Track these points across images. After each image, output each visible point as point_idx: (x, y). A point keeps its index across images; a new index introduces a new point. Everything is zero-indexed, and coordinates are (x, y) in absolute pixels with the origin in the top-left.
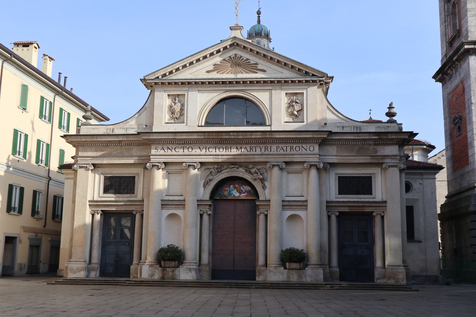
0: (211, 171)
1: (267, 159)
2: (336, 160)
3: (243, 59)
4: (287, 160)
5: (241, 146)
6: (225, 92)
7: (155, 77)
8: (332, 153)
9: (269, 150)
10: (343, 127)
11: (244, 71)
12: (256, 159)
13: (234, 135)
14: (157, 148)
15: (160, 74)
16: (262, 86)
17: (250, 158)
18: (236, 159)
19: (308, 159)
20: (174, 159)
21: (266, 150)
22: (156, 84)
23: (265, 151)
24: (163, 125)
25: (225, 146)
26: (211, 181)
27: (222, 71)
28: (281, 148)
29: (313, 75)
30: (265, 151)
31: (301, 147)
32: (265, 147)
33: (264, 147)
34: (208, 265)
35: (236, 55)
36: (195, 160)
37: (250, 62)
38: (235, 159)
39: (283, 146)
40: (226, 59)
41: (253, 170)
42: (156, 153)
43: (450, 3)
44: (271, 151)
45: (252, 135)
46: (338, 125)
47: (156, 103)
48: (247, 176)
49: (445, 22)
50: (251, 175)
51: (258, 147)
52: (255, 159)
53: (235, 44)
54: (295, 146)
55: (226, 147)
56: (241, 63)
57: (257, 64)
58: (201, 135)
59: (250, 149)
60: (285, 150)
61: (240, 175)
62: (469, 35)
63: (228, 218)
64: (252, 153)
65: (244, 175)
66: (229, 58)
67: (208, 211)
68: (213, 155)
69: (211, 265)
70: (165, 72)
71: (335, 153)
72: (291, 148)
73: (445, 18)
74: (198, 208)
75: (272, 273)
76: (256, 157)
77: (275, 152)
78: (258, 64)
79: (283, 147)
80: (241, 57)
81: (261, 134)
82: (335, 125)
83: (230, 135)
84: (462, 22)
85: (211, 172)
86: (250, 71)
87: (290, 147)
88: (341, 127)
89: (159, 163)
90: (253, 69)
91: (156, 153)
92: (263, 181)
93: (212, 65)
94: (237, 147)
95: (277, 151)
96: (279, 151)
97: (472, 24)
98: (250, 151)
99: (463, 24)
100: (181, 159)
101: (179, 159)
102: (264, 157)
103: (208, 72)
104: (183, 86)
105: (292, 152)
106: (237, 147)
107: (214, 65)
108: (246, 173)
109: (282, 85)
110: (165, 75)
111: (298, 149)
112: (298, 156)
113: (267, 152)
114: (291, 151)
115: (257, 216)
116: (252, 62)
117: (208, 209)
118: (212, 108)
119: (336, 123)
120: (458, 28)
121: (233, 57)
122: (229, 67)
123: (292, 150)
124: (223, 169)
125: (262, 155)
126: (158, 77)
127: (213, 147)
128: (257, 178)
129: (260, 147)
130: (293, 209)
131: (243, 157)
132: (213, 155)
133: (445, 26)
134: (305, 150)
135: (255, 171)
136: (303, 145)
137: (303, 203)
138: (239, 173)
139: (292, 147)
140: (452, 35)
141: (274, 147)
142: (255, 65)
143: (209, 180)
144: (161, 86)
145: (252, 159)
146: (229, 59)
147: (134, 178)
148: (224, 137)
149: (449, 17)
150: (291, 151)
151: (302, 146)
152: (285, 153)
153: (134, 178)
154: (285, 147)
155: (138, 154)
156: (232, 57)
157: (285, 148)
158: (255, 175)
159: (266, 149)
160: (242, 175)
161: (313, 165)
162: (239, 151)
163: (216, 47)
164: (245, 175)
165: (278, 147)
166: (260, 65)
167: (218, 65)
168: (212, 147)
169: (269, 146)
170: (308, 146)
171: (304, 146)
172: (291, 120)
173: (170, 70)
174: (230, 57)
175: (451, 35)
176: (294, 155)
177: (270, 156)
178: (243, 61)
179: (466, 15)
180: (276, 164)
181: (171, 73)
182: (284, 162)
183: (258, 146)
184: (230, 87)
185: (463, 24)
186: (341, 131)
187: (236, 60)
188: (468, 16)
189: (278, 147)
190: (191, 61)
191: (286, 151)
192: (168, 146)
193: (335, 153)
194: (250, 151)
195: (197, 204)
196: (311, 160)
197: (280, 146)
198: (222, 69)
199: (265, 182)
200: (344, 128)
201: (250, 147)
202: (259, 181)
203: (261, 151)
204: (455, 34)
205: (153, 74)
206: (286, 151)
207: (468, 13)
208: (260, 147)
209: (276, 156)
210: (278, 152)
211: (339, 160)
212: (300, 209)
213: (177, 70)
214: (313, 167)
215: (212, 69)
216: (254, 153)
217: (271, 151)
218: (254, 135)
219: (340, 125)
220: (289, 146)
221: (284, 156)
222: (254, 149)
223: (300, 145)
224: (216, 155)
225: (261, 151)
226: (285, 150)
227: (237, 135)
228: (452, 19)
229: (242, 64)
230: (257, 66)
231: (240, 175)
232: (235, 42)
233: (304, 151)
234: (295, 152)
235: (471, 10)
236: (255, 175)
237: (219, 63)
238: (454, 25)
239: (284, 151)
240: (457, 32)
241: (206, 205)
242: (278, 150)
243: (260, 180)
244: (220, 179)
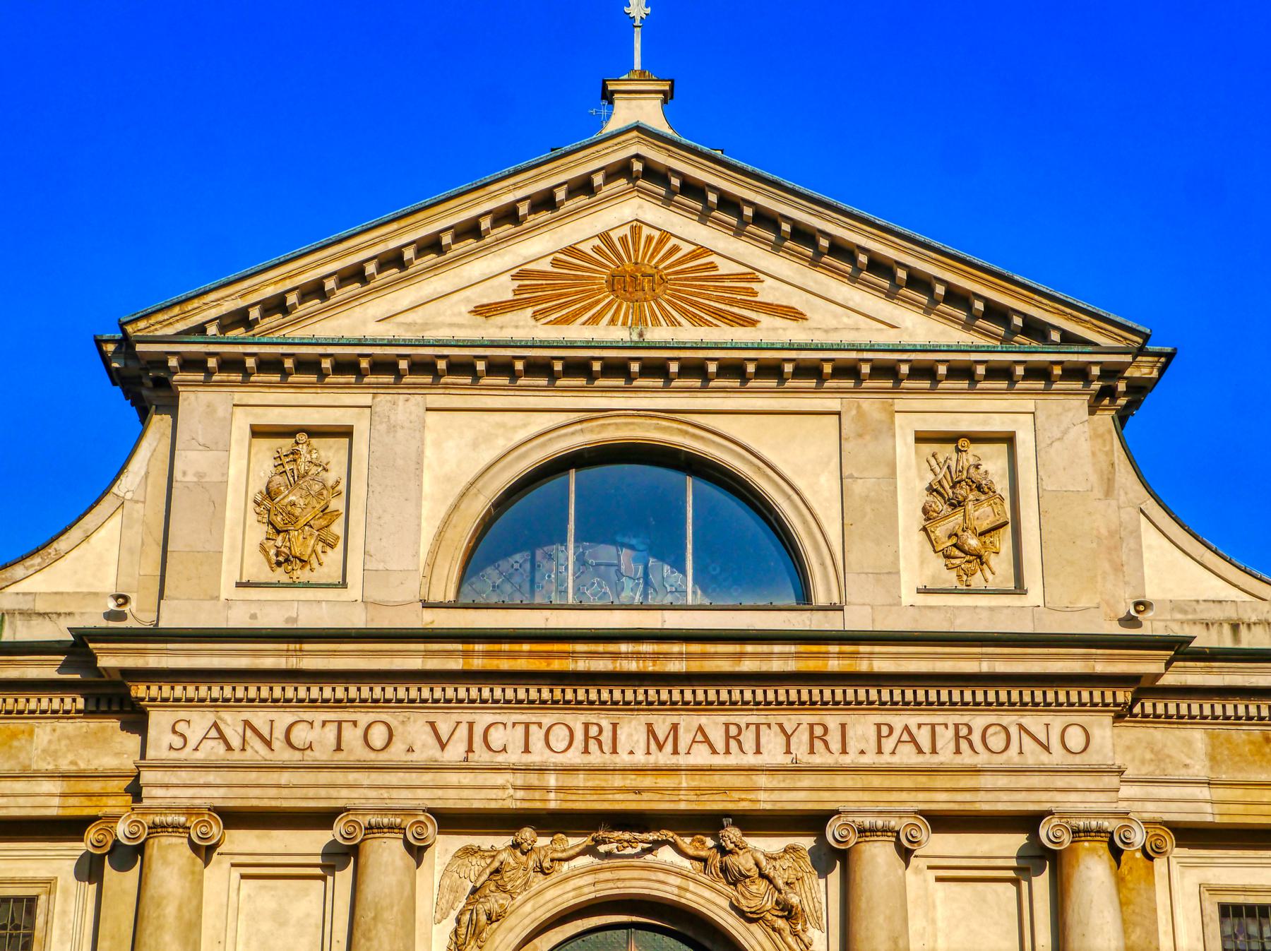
0: (496, 864)
1: (826, 795)
2: (1208, 808)
3: (675, 249)
4: (942, 802)
5: (675, 719)
6: (581, 422)
7: (181, 326)
8: (1186, 766)
9: (835, 745)
10: (1235, 627)
11: (684, 313)
12: (762, 796)
13: (638, 656)
14: (181, 727)
15: (213, 313)
17: (725, 790)
18: (645, 796)
19: (1059, 797)
20: (285, 792)
21: (818, 745)
22: (192, 363)
23: (812, 752)
24: (223, 596)
26: (495, 925)
27: (561, 306)
28: (906, 737)
29: (1068, 338)
30: (812, 752)
31: (1014, 731)
32: (811, 726)
33: (804, 727)
35: (636, 231)
36: (404, 798)
37: (715, 267)
38: (638, 791)
39: (912, 720)
40: (586, 248)
42: (174, 755)
44: (844, 751)
46: (1207, 616)
47: (184, 473)
48: (708, 894)
50: (729, 890)
51: (769, 726)
52: (752, 796)
53: (638, 166)
54: (979, 721)
55: (587, 726)
56: (665, 268)
57: (753, 275)
59: (728, 737)
60: (926, 745)
64: (734, 760)
65: (686, 890)
66: (597, 242)
68: (514, 770)
70: (241, 303)
71: (1200, 769)
72: (957, 737)
76: (762, 780)
77: (870, 759)
78: (761, 276)
79: (914, 730)
80: (666, 235)
82: (1190, 617)
85: (497, 871)
86: (719, 315)
87: (951, 732)
88: (1227, 629)
89: (189, 811)
90: (732, 302)
91: (174, 755)
92: (799, 927)
93: (507, 277)
94: (649, 725)
95: (880, 752)
96: (893, 753)
98: (728, 752)
100: (323, 792)
101: (311, 792)
102: (807, 781)
103: (484, 311)
105: (967, 759)
106: (649, 725)
107: (515, 278)
108: (702, 878)
109: (896, 388)
110: (240, 318)
111: (996, 742)
112: (1002, 781)
113: (820, 759)
114: (958, 751)
116: (725, 267)
118: (487, 524)
119: (1198, 601)
121: (623, 240)
122: (600, 290)
123: (964, 745)
125: (797, 770)
126: (201, 329)
127: (514, 724)
129: (781, 726)
131: (684, 785)
132: (514, 770)
134: (1039, 748)
138: (661, 876)
139: (964, 731)
141: (863, 727)
142: (741, 280)
143: (483, 918)
145: (736, 795)
146: (597, 249)
147: (32, 901)
150: (958, 751)
151: (1021, 727)
152: (927, 760)
153: (32, 901)
154: (926, 731)
155: (64, 765)
156: (615, 235)
157: (923, 737)
159: (817, 738)
160: (676, 891)
161: (1087, 831)
162: (660, 747)
163: (535, 179)
164: (692, 886)
165: (885, 731)
166: (769, 282)
167: (543, 275)
168: (505, 725)
169: (833, 721)
170: (1057, 722)
171: (1034, 722)
172: (951, 579)
173: (270, 291)
174: (605, 237)
176: (976, 771)
177: (839, 781)
178: (679, 262)
180: (880, 823)
181: (276, 305)
182: (921, 813)
183: (773, 718)
186: (1228, 643)
187: (636, 251)
189: (885, 731)
190: (393, 244)
191: (934, 751)
193: (1200, 769)
194: (728, 752)
196: (1072, 802)
197: (898, 721)
198: (560, 296)
199: (809, 934)
200: (1243, 629)
201: (727, 725)
203: (788, 752)
205: (176, 310)
206: (934, 751)
208: (781, 726)
209: (876, 781)
210: (886, 759)
211: (1225, 808)
213: (315, 290)
215: (510, 296)
216: (750, 759)
217: (844, 751)
218: (755, 655)
219: (1216, 613)
220: (946, 726)
221: (923, 781)
222: (748, 738)
223: (1009, 719)
224: (527, 769)
225: (788, 752)
226: (926, 745)
227: (656, 656)
229: (669, 274)
230: (754, 286)
231: (668, 889)
232: (638, 157)
233: (1034, 756)
234: (982, 759)
236: (753, 888)
237: (549, 268)
239: (920, 751)
242: (888, 745)
244: (548, 915)
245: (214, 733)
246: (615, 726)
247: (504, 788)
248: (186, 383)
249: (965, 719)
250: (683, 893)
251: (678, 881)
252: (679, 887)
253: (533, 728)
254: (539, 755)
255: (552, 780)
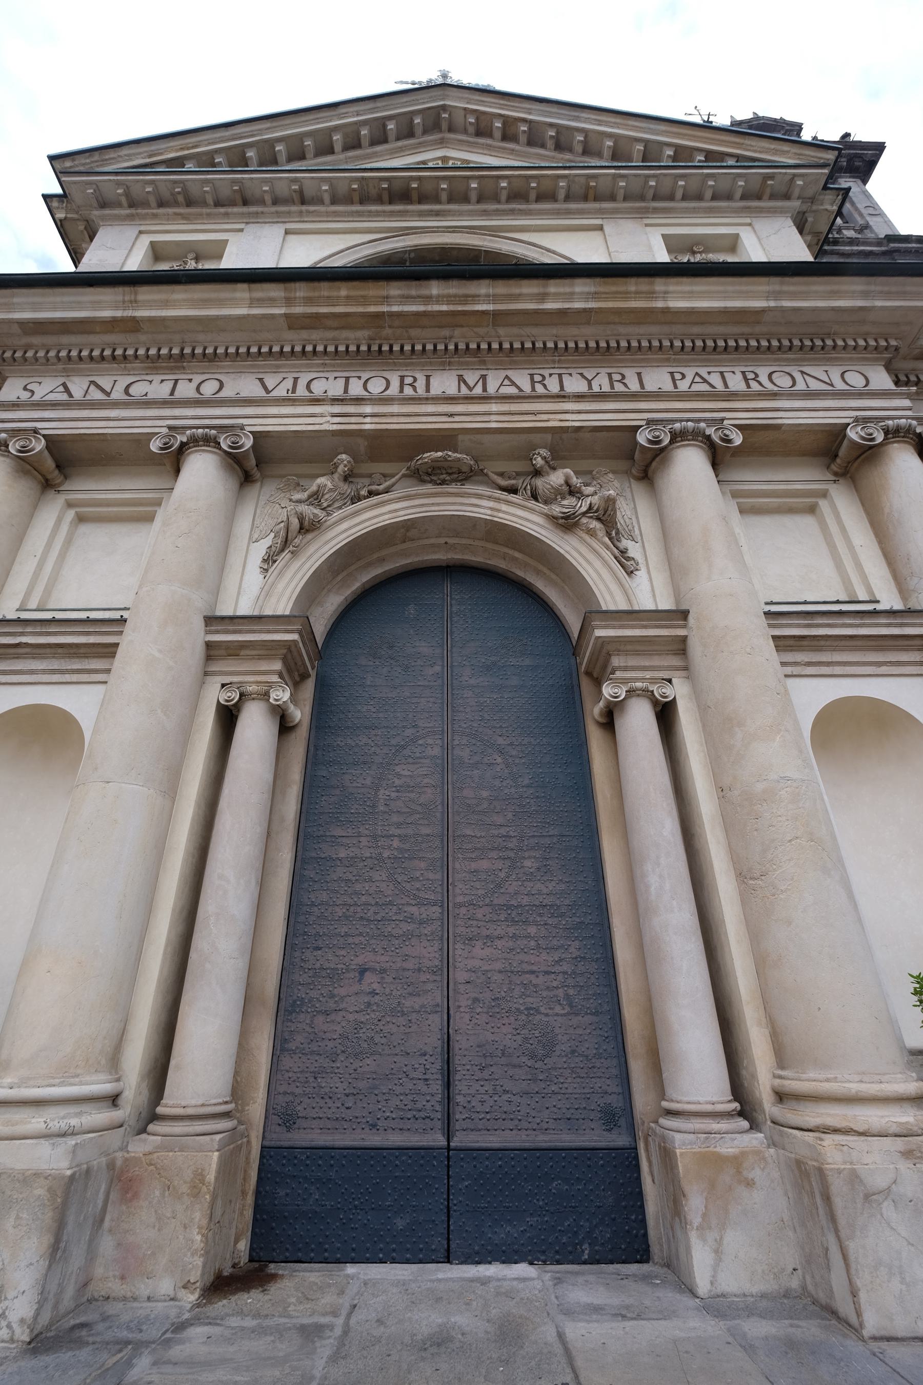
12: (568, 417)
16: (558, 213)
18: (457, 419)
20: (112, 424)
25: (400, 373)
26: (309, 536)
34: (226, 1115)
41: (556, 478)
45: (543, 297)
48: (520, 512)
51: (570, 374)
55: (402, 378)
58: (271, 301)
61: (482, 511)
63: (407, 752)
65: (499, 511)
67: (270, 685)
69: (257, 1109)
74: (206, 674)
75: (887, 1208)
81: (593, 289)
83: (428, 299)
104: (222, 210)
115: (596, 738)
117: (275, 678)
124: (381, 487)
128: (584, 509)
130: (838, 670)
135: (567, 483)
136: (805, 369)
137: (902, 625)
143: (295, 522)
144: (128, 211)
148: (395, 309)
151: (802, 372)
158: (569, 501)
164: (504, 507)
165: (678, 376)
184: (422, 215)
192: (92, 378)
195: (209, 645)
202: (594, 524)
212: (884, 670)
214: (895, 445)
218: (557, 296)
241: (267, 650)
243: (598, 519)
245: (61, 389)
246: (428, 377)
247: (322, 416)
248: (104, 218)
249: (751, 369)
250: (495, 514)
251: (491, 504)
252: (491, 509)
253: (351, 380)
254: (356, 389)
255: (368, 409)
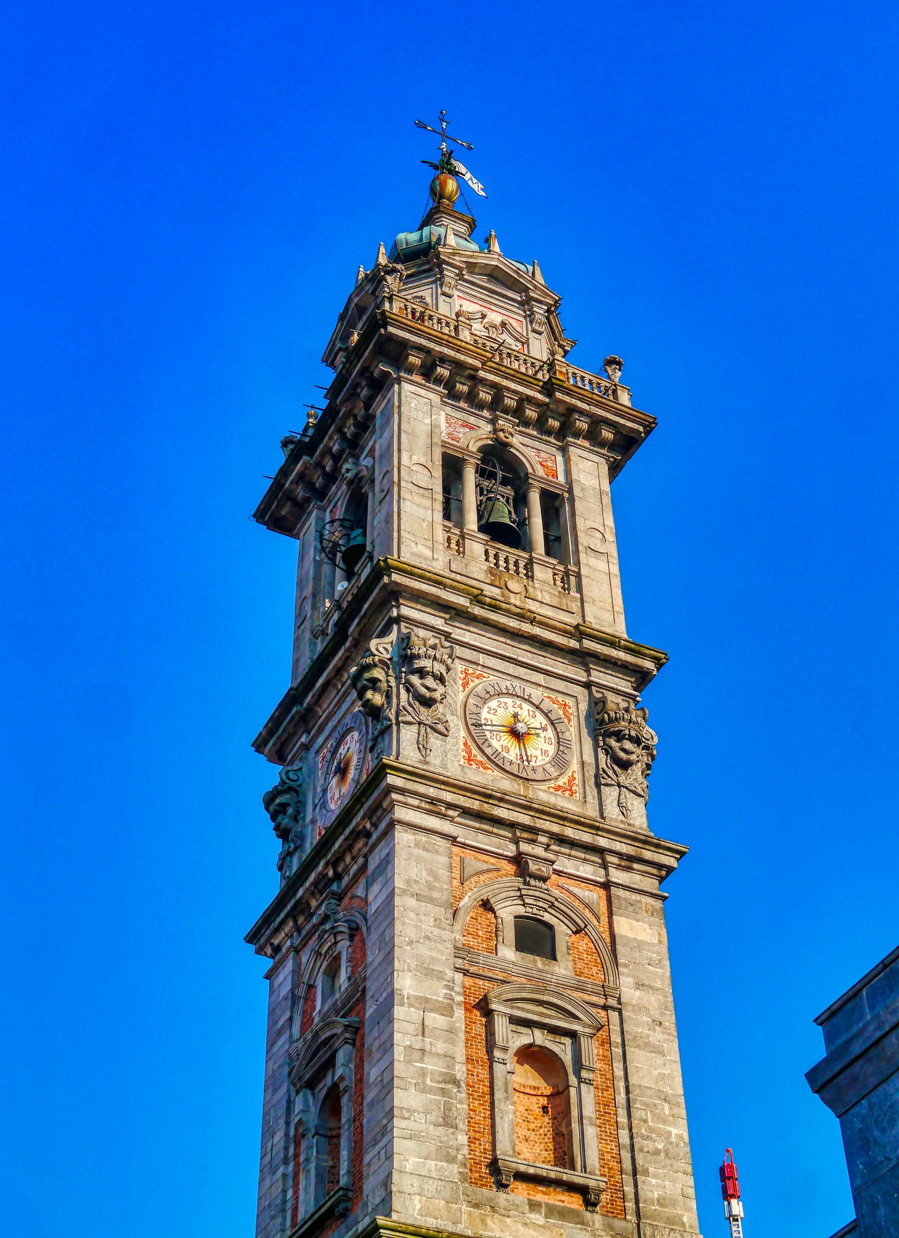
43: (313, 1095)
49: (286, 1161)
62: (396, 1204)
73: (286, 1148)
84: (367, 1159)
97: (409, 1167)
99: (369, 1164)
120: (343, 1181)
133: (284, 1176)
140: (311, 1211)
149: (304, 1144)
175: (306, 1212)
179: (386, 1131)
185: (369, 1164)
188: (396, 1132)
204: (329, 1203)
207: (396, 1122)
228: (317, 1152)
235: (406, 1115)
238: (329, 1175)
240: (341, 1193)
